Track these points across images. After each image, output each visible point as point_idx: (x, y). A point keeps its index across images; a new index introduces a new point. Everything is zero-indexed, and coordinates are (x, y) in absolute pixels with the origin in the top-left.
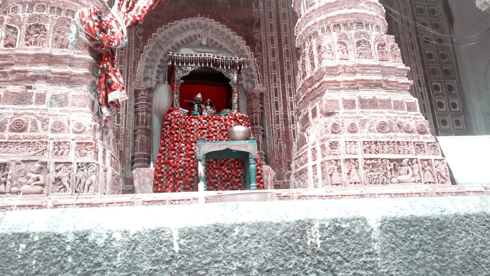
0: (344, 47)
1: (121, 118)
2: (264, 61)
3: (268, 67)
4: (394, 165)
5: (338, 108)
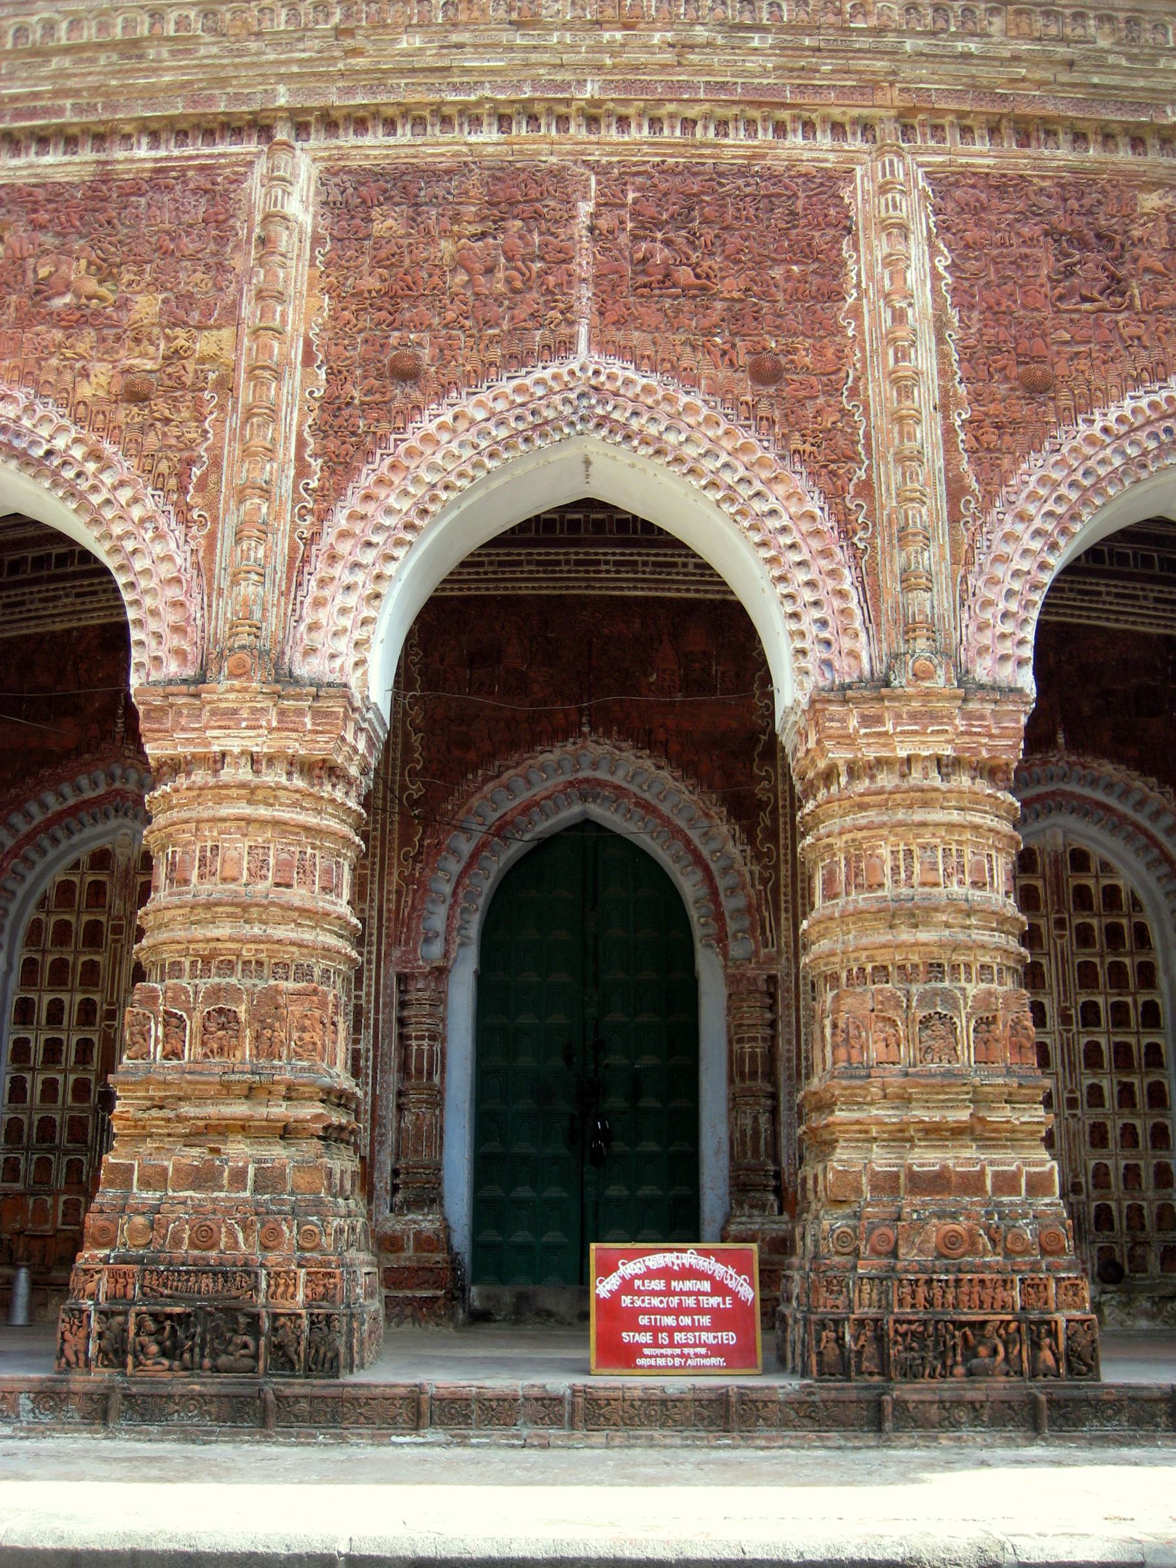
0: (892, 1031)
1: (362, 1063)
2: (783, 873)
3: (794, 892)
4: (965, 1335)
5: (858, 1191)
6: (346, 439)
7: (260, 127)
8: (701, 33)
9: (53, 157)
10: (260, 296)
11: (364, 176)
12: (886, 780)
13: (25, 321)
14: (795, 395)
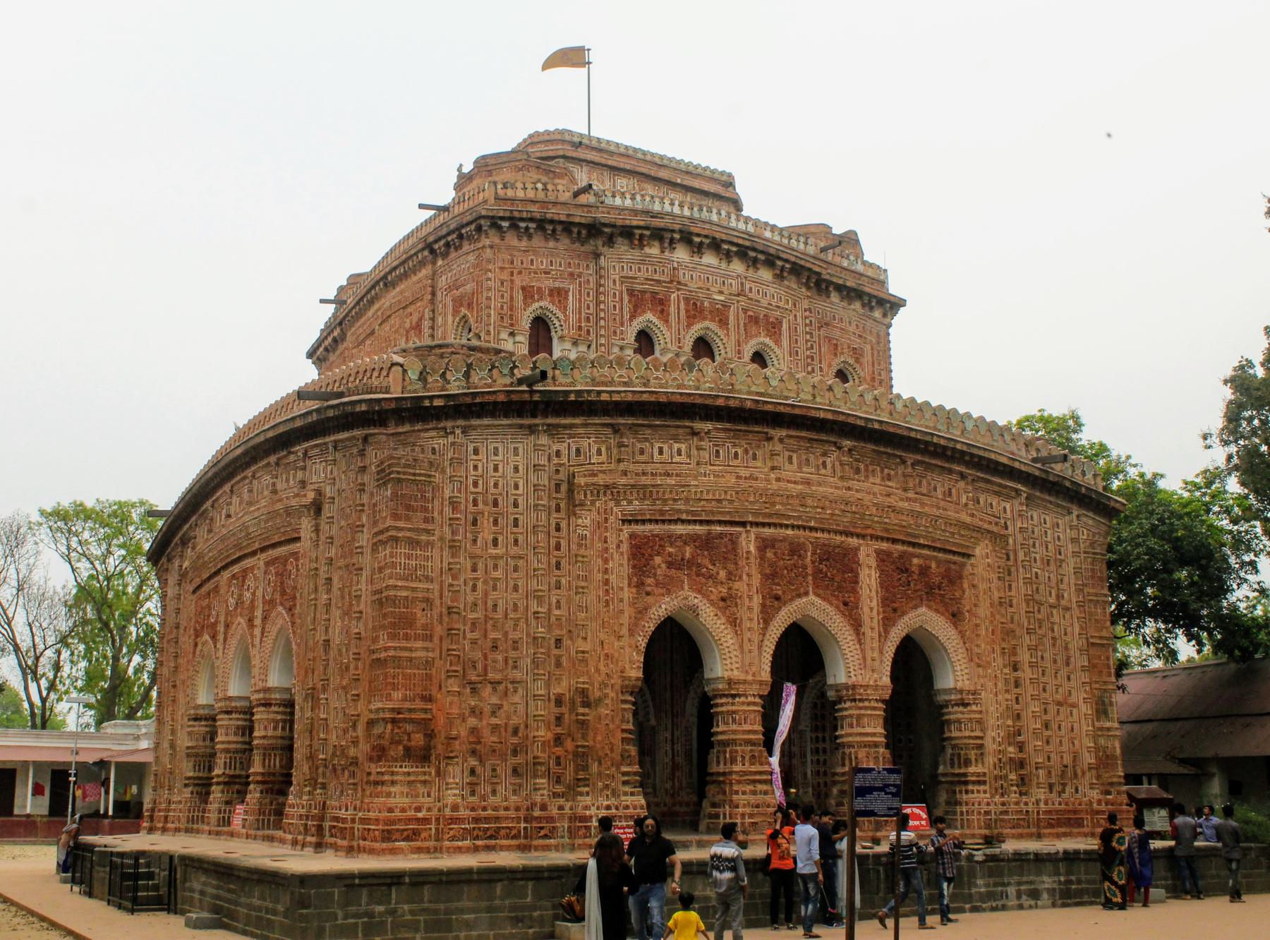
6: (766, 617)
7: (743, 524)
8: (837, 512)
9: (698, 527)
10: (748, 575)
11: (764, 540)
12: (866, 704)
13: (698, 575)
14: (850, 609)
